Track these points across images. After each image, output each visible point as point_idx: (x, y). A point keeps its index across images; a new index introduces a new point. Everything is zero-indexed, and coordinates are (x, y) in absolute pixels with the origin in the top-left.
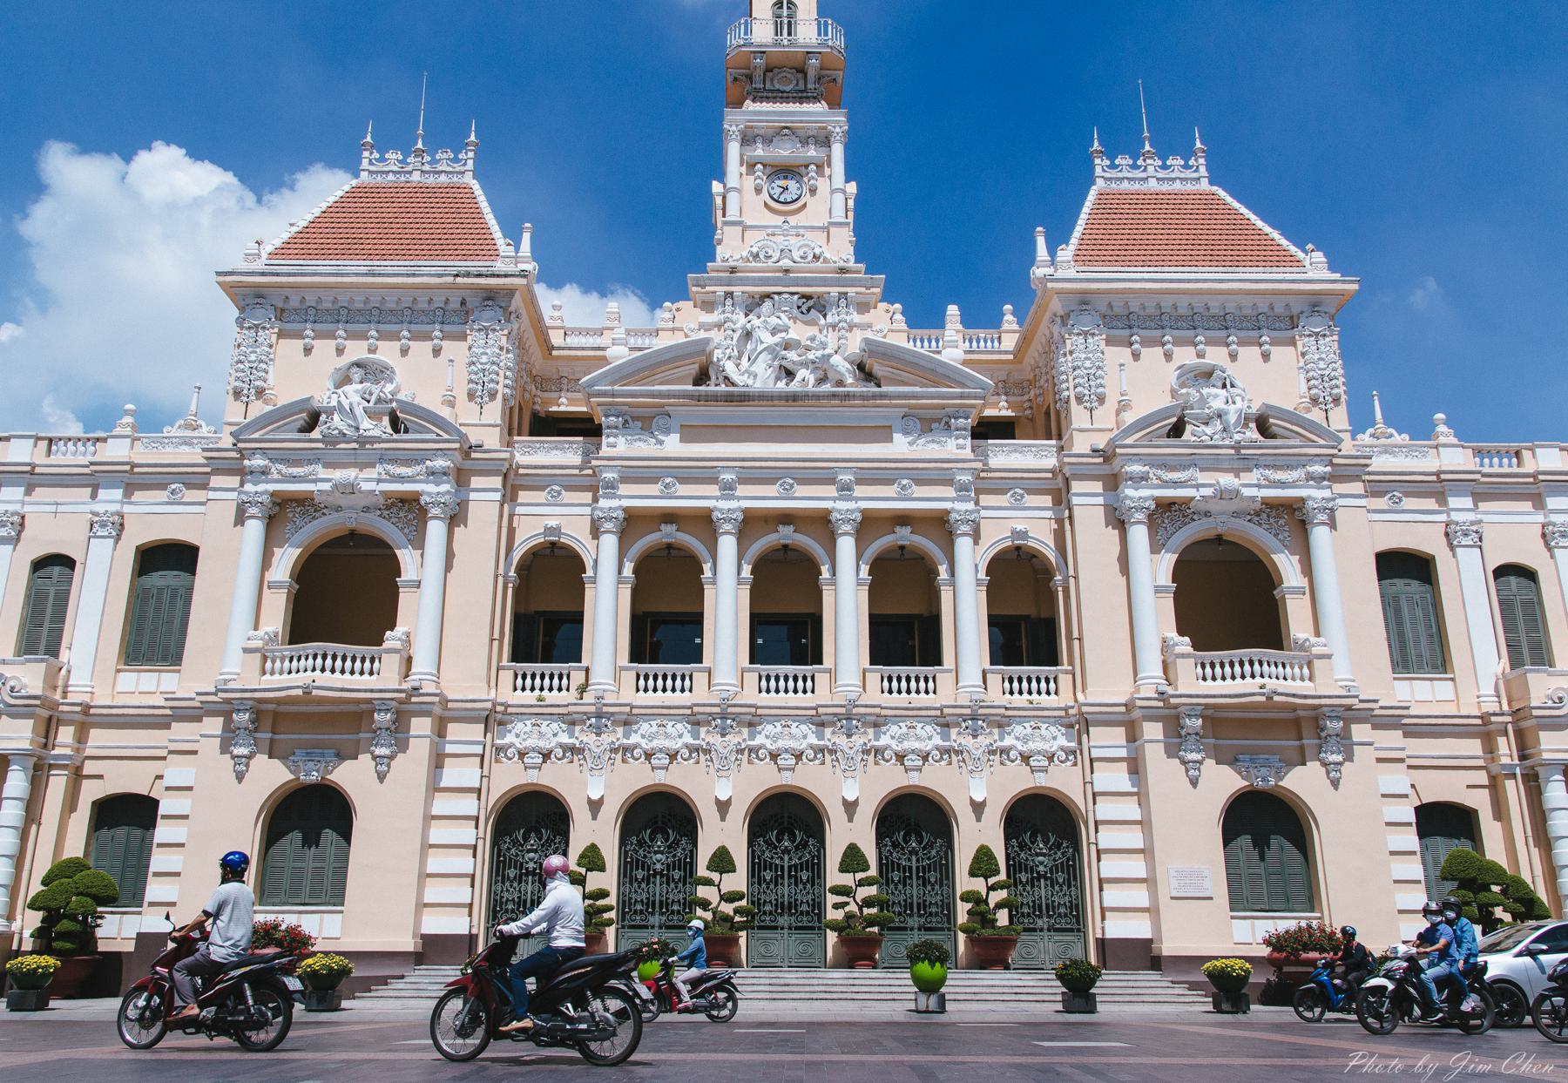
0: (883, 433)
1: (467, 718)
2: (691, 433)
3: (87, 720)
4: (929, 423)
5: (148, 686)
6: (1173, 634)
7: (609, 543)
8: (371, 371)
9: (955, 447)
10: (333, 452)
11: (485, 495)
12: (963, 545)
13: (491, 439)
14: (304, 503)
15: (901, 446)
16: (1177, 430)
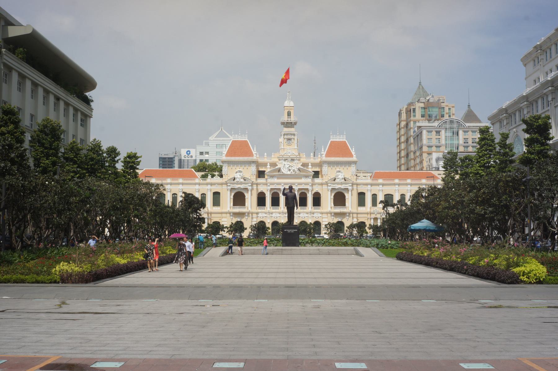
0: (301, 178)
1: (254, 213)
2: (278, 178)
3: (211, 213)
4: (307, 177)
5: (216, 209)
6: (332, 204)
7: (269, 192)
8: (240, 172)
9: (309, 180)
10: (238, 183)
11: (255, 187)
12: (310, 192)
13: (254, 181)
14: (234, 189)
15: (303, 180)
16: (334, 180)
